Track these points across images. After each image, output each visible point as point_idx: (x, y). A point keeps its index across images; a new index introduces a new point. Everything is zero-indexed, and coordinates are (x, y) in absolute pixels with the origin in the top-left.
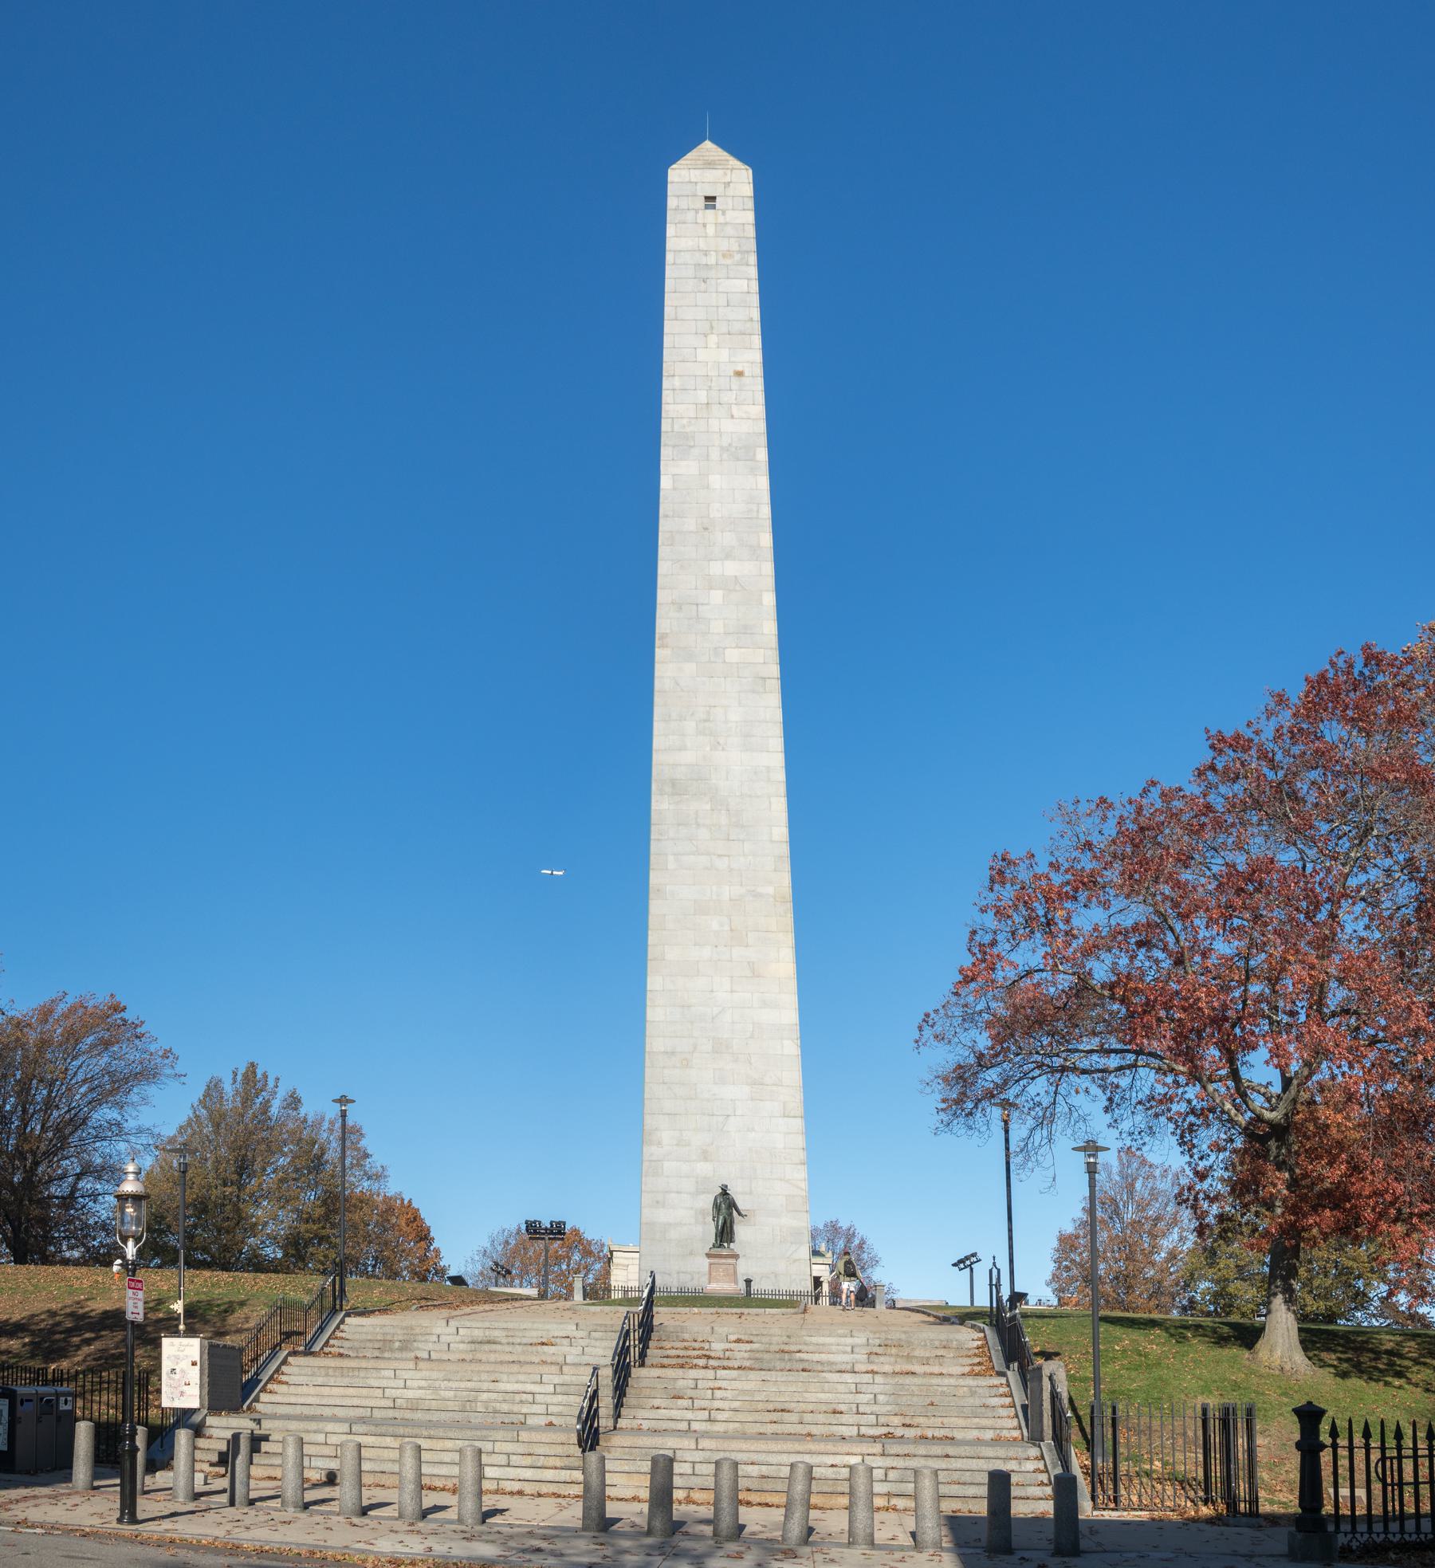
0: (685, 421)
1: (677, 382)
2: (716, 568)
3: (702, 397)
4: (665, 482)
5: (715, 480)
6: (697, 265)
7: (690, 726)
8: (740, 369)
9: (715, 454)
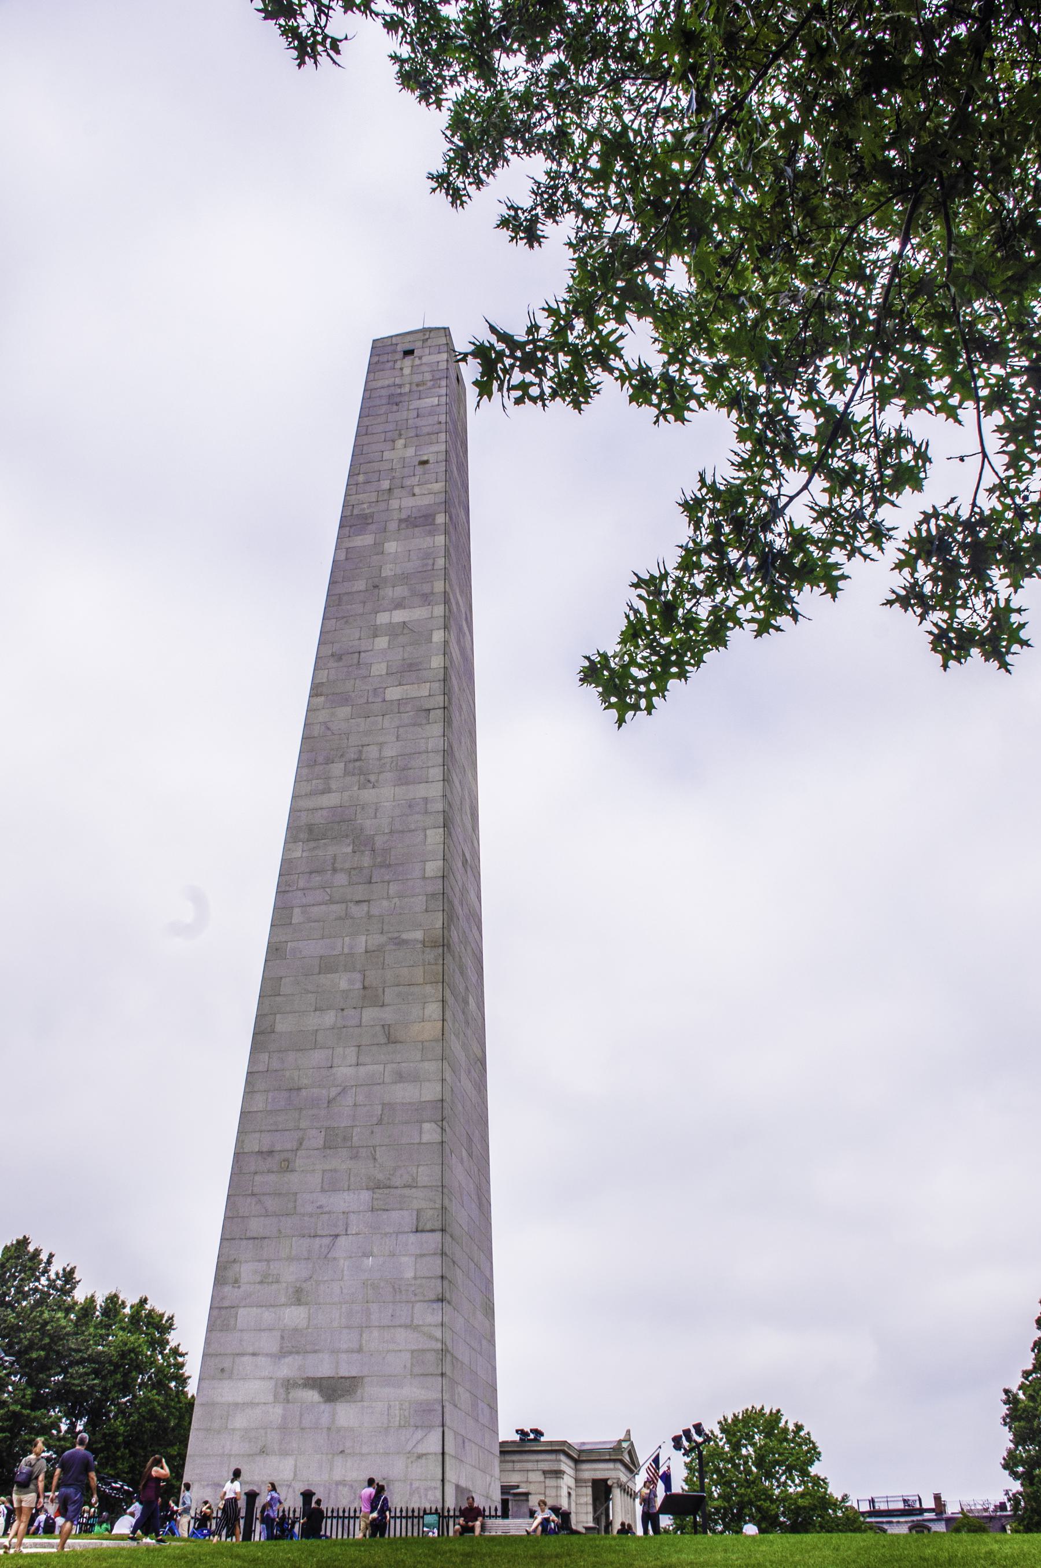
0: (365, 506)
2: (383, 618)
3: (386, 485)
7: (337, 768)
8: (425, 458)
9: (393, 526)
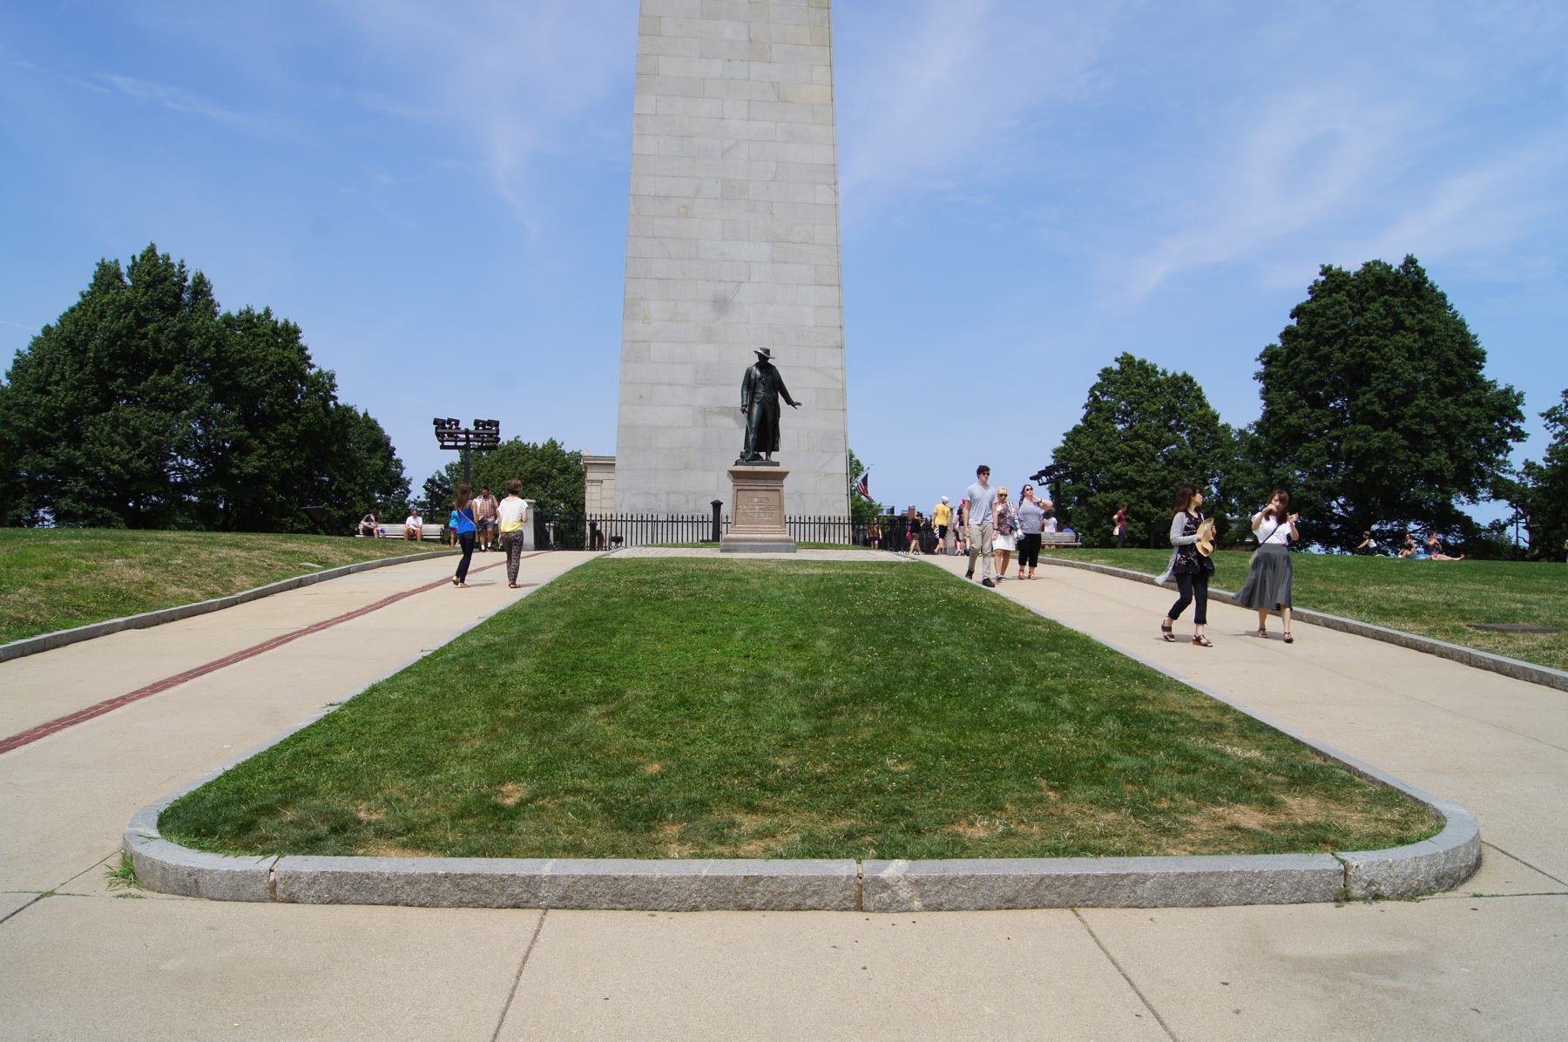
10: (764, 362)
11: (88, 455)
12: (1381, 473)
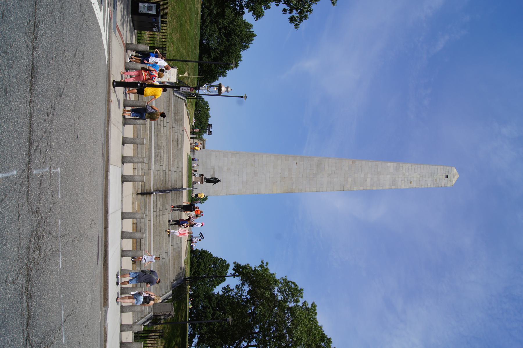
1: (410, 168)
2: (369, 176)
3: (407, 174)
4: (389, 164)
5: (388, 176)
6: (434, 173)
10: (219, 181)
11: (207, 26)
12: (202, 316)
